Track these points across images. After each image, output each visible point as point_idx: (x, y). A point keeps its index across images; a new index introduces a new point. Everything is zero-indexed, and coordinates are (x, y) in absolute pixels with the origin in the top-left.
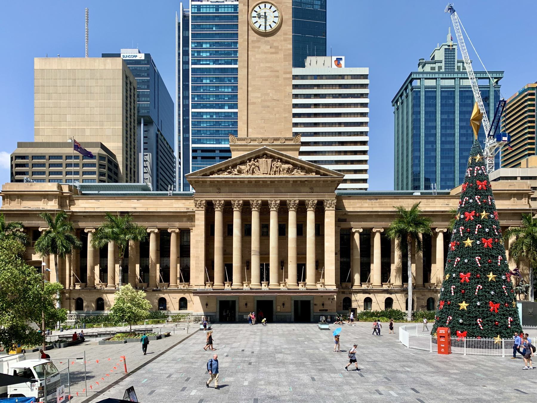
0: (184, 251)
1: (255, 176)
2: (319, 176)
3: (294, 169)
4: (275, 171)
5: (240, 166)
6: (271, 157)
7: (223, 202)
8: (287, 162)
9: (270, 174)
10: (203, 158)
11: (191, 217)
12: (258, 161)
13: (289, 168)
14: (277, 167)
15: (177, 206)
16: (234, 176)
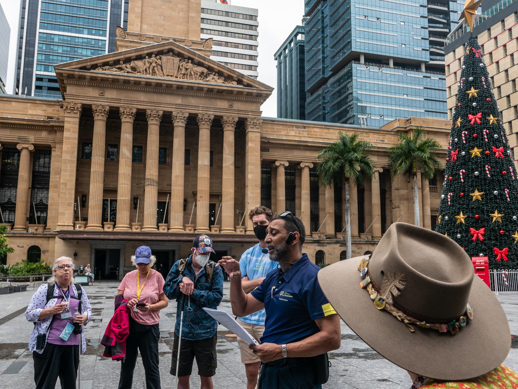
0: (40, 180)
1: (155, 77)
2: (242, 86)
3: (209, 74)
4: (184, 74)
5: (136, 62)
6: (179, 55)
7: (107, 108)
8: (200, 64)
9: (176, 77)
10: (50, 89)
11: (56, 129)
12: (160, 59)
13: (203, 73)
14: (187, 69)
15: (34, 113)
16: (126, 74)
